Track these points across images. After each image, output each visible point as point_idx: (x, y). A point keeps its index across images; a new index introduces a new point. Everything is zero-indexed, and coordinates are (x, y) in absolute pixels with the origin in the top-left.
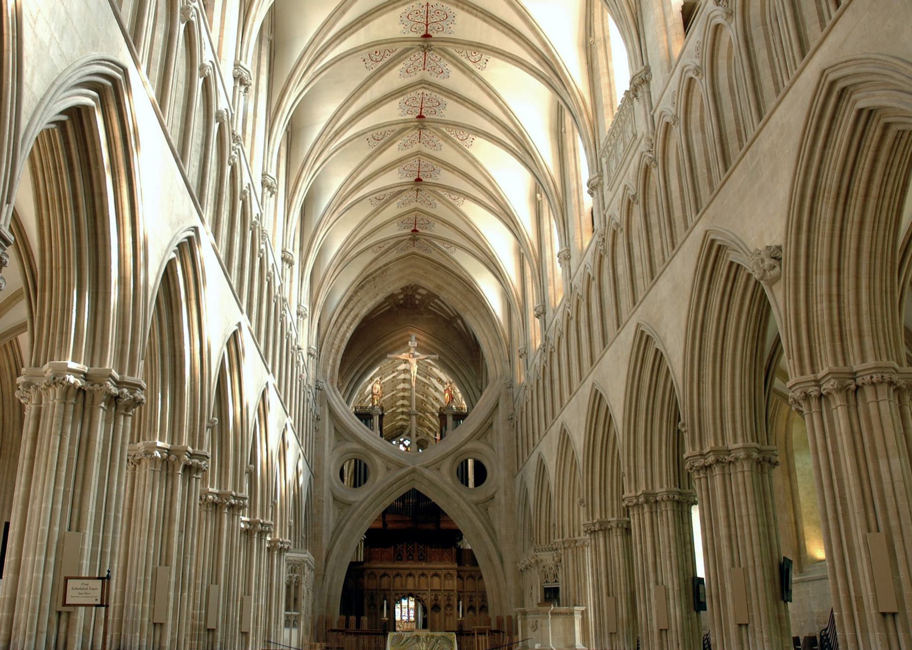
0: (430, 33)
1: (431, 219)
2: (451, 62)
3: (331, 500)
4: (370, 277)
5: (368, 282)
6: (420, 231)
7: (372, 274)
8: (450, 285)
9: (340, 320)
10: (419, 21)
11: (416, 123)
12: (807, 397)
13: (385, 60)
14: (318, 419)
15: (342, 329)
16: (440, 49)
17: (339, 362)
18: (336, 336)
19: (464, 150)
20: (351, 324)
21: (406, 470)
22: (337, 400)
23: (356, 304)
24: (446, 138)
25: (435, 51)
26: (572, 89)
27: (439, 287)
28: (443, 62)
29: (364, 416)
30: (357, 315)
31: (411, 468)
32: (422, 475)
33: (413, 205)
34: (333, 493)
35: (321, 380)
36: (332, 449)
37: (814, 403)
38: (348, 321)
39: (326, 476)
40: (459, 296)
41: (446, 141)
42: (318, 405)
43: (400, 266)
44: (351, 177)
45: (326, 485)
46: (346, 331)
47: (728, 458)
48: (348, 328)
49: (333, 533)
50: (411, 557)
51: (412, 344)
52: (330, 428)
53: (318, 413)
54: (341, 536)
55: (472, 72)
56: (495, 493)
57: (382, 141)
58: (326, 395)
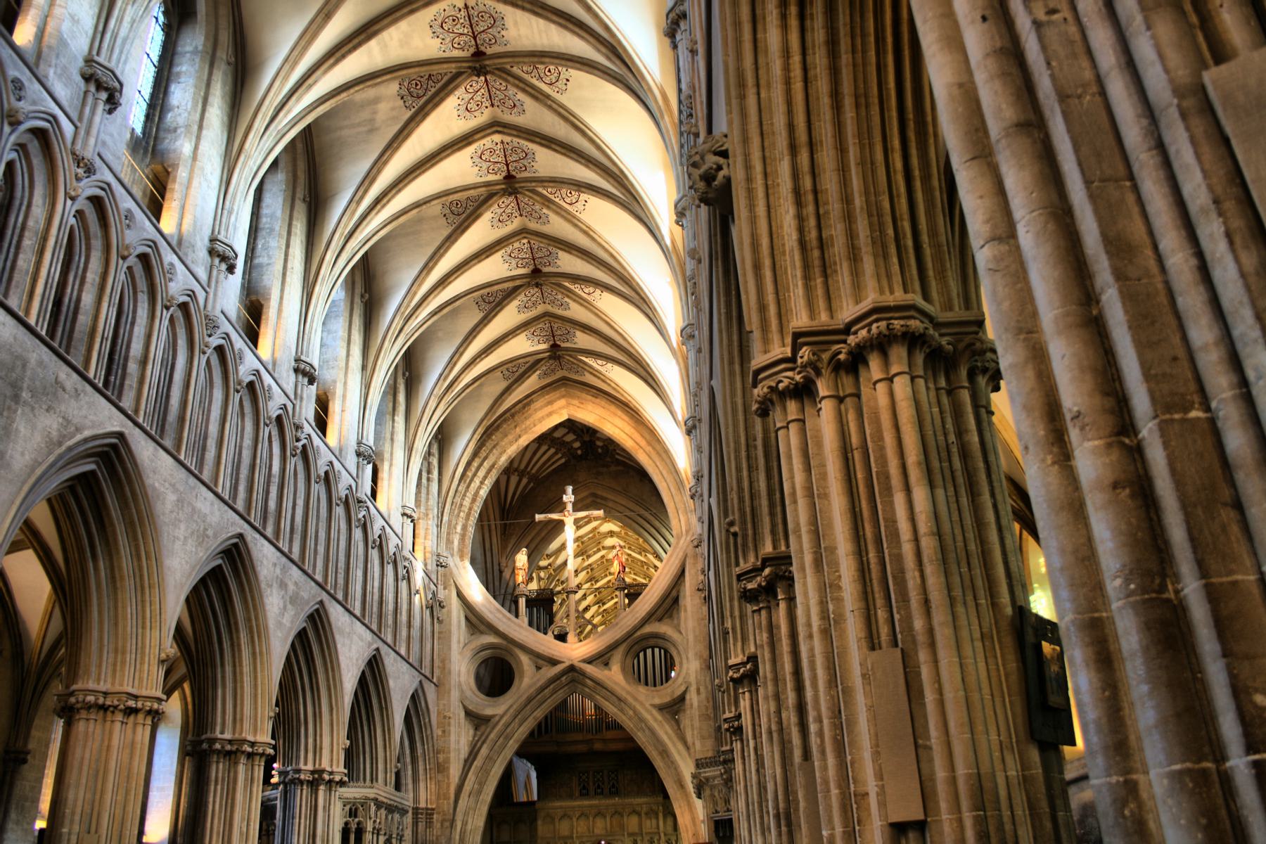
0: (482, 48)
1: (568, 326)
2: (517, 87)
3: (462, 714)
4: (508, 415)
6: (563, 345)
9: (470, 474)
10: (461, 31)
11: (503, 186)
13: (430, 94)
15: (472, 485)
16: (498, 69)
18: (465, 495)
19: (574, 217)
20: (485, 478)
21: (559, 668)
23: (491, 451)
24: (548, 202)
25: (493, 73)
26: (648, 84)
28: (512, 91)
30: (493, 466)
31: (567, 664)
32: (583, 673)
34: (465, 707)
35: (445, 554)
36: (462, 645)
38: (481, 473)
39: (453, 682)
41: (548, 208)
46: (480, 488)
48: (482, 483)
49: (466, 761)
50: (599, 792)
51: (569, 497)
54: (475, 763)
55: (548, 97)
56: (685, 692)
57: (464, 215)
58: (451, 573)
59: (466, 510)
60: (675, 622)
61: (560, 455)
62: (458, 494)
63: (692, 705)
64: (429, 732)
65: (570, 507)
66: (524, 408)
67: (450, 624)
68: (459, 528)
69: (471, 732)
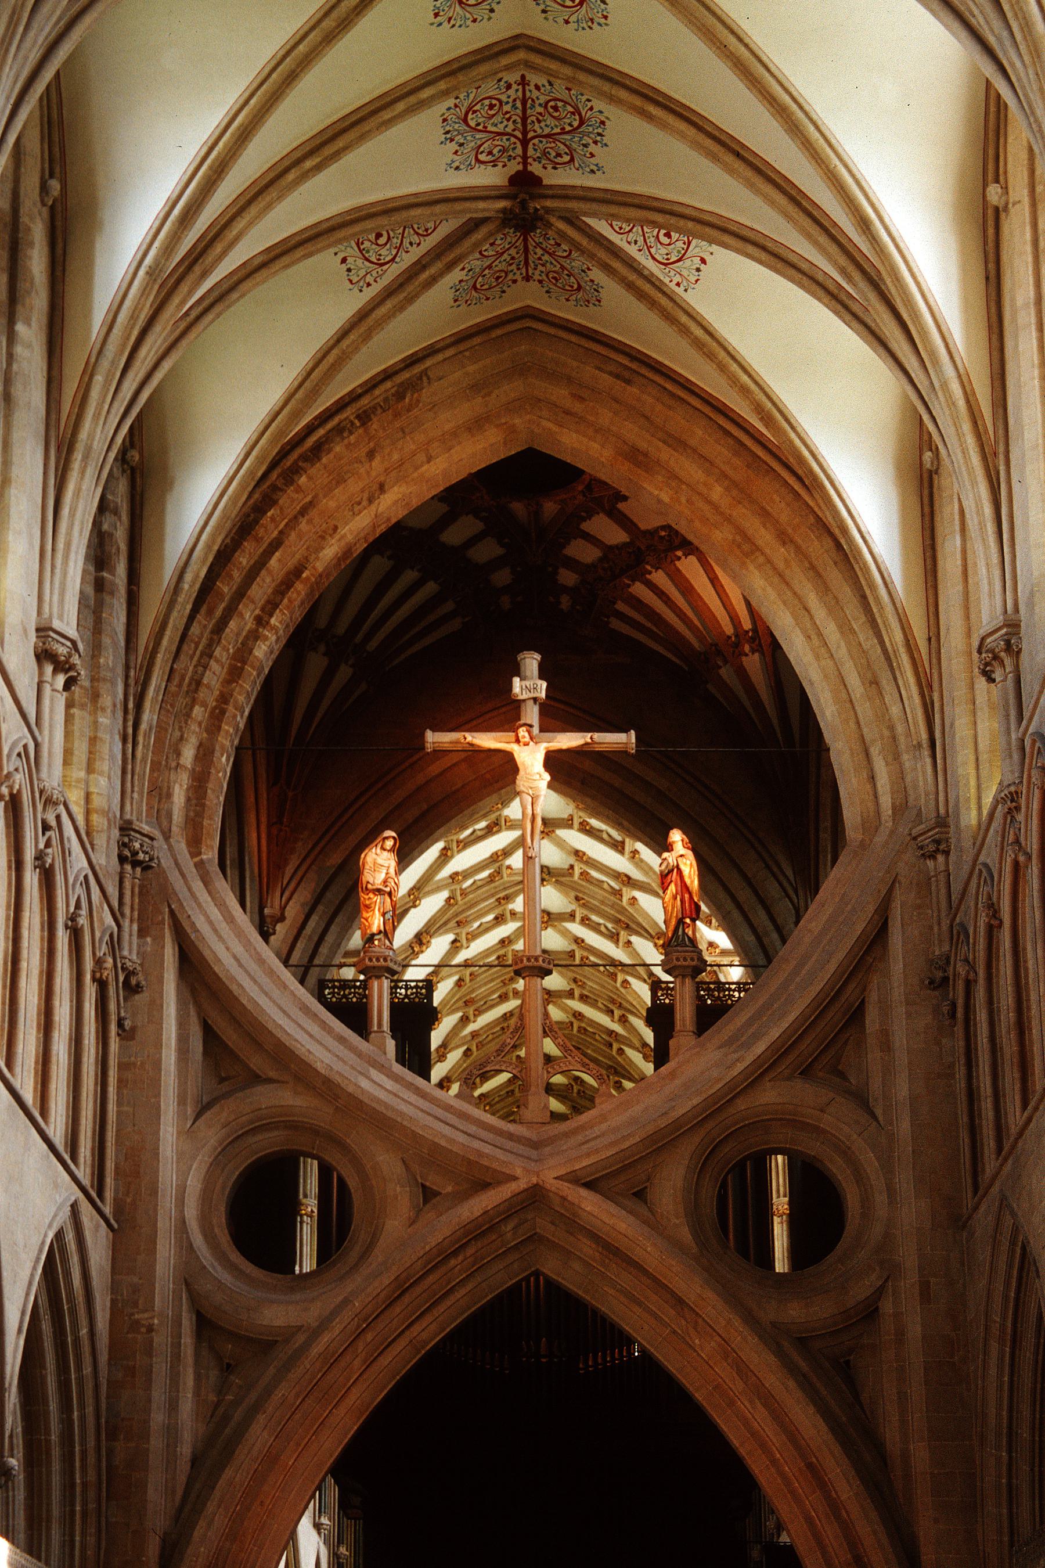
4: (349, 413)
5: (339, 430)
7: (353, 397)
9: (226, 588)
14: (131, 989)
15: (232, 624)
17: (224, 763)
18: (208, 654)
20: (271, 606)
21: (507, 1191)
30: (297, 572)
35: (146, 828)
38: (261, 590)
39: (165, 1224)
42: (130, 928)
43: (471, 369)
48: (260, 621)
52: (182, 1025)
59: (212, 703)
61: (449, 606)
62: (188, 648)
64: (87, 1370)
65: (536, 709)
66: (400, 396)
67: (158, 1045)
68: (188, 754)
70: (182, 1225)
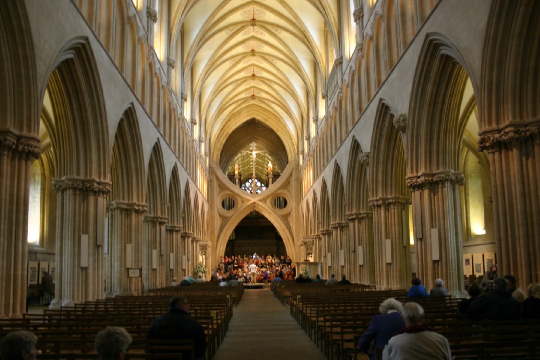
4: (233, 116)
8: (270, 118)
12: (374, 205)
22: (219, 172)
25: (257, 26)
27: (265, 119)
28: (261, 30)
29: (231, 177)
30: (227, 133)
32: (258, 205)
33: (252, 85)
36: (218, 193)
37: (376, 207)
40: (275, 124)
42: (211, 175)
44: (222, 78)
45: (216, 209)
47: (360, 216)
53: (211, 178)
60: (288, 189)
63: (293, 216)
69: (221, 221)
70: (217, 206)
